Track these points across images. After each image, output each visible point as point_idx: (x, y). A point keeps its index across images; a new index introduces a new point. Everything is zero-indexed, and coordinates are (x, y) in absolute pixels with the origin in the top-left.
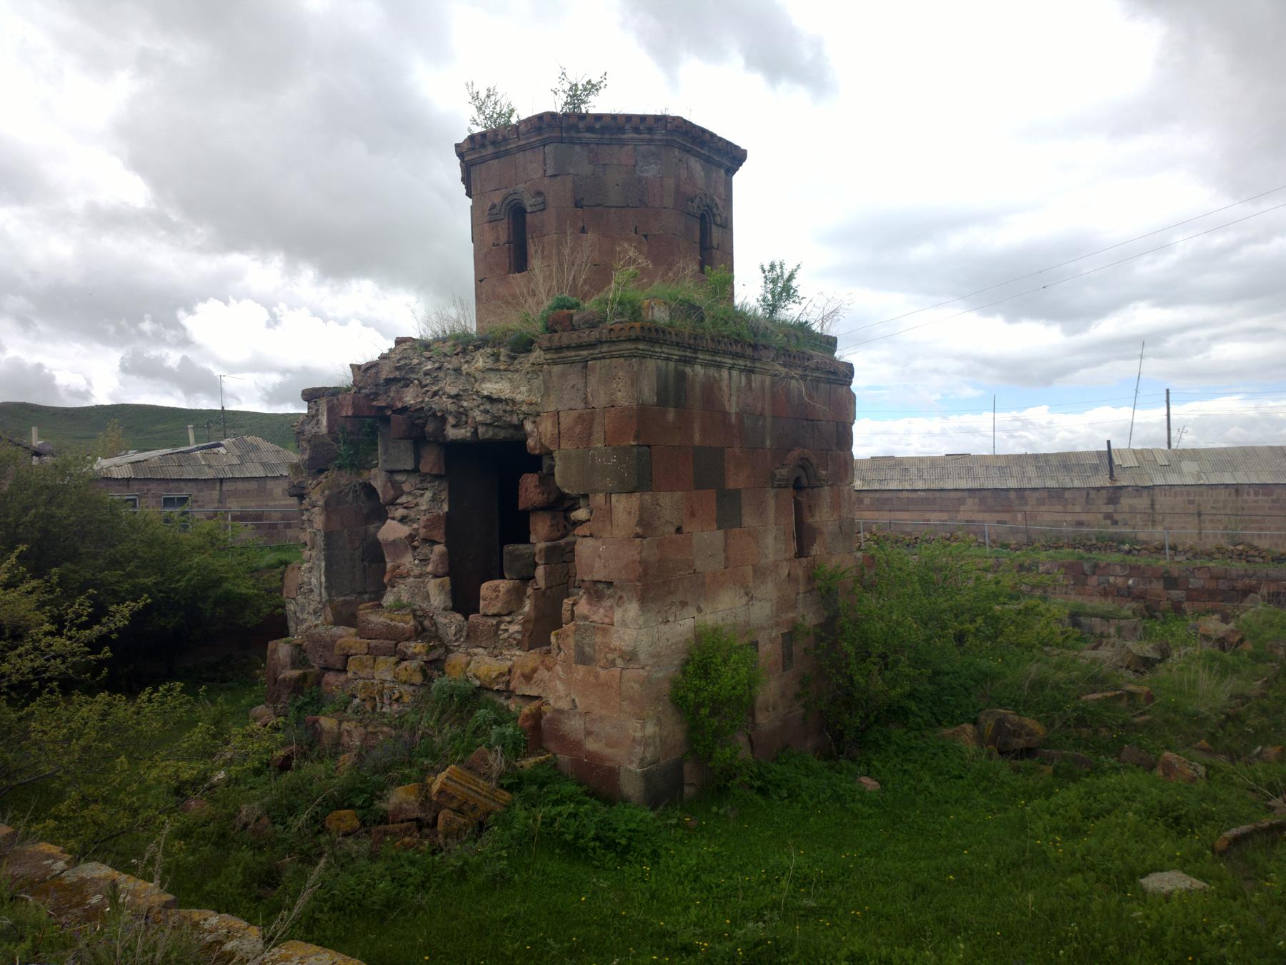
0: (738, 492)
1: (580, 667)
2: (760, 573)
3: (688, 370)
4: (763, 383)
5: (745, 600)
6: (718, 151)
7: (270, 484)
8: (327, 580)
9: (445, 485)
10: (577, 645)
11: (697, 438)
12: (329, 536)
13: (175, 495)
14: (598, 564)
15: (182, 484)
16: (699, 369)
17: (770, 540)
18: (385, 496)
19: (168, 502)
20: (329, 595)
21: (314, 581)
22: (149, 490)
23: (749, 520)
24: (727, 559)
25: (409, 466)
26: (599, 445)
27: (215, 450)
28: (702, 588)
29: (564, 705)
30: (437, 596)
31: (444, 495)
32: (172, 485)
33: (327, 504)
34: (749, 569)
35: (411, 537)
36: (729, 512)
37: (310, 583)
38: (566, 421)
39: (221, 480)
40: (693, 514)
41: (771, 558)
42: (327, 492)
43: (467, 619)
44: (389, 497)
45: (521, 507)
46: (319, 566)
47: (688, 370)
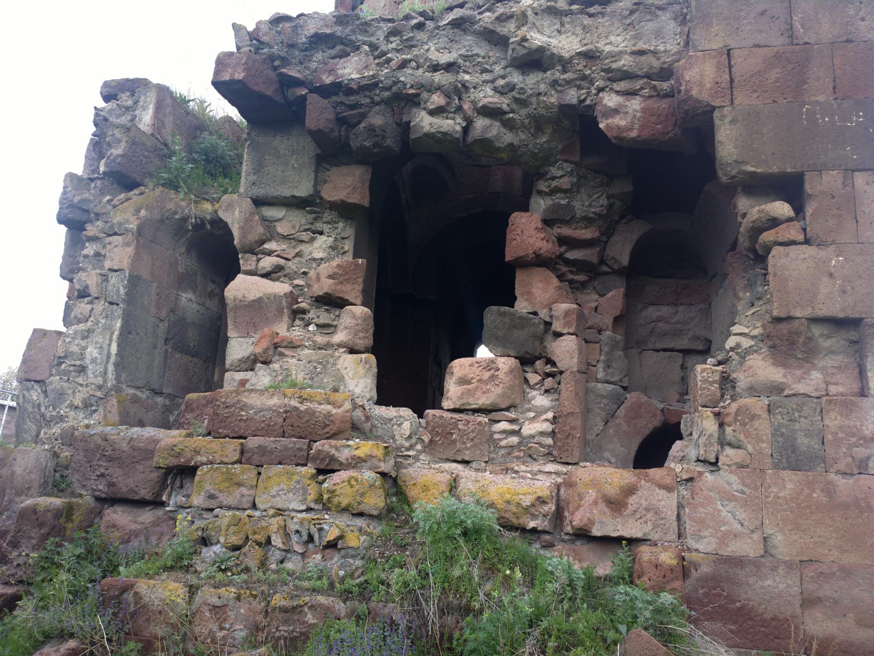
1: (787, 474)
8: (119, 354)
9: (350, 232)
10: (776, 432)
12: (134, 281)
14: (825, 288)
18: (243, 236)
20: (118, 378)
21: (92, 351)
25: (303, 190)
26: (821, 98)
29: (746, 547)
30: (358, 377)
31: (348, 246)
33: (140, 232)
35: (292, 298)
37: (82, 357)
38: (743, 64)
42: (143, 213)
43: (420, 416)
44: (253, 237)
45: (508, 258)
46: (108, 328)
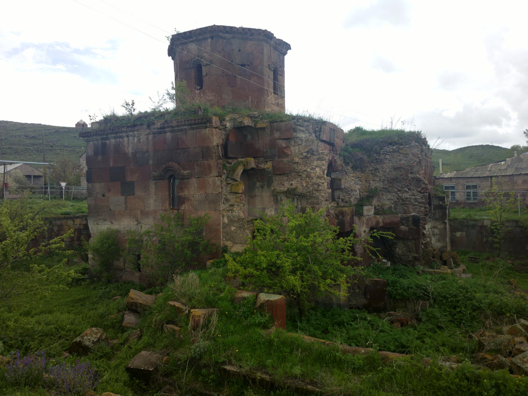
0: (132, 183)
2: (145, 214)
3: (107, 142)
4: (147, 139)
5: (136, 223)
6: (200, 34)
7: (515, 178)
11: (111, 164)
13: (471, 184)
15: (474, 179)
16: (113, 141)
17: (152, 201)
19: (468, 187)
22: (459, 182)
23: (138, 192)
24: (126, 207)
27: (499, 163)
28: (113, 216)
32: (469, 180)
34: (139, 211)
36: (127, 189)
39: (491, 177)
40: (109, 190)
41: (152, 208)
47: (107, 142)
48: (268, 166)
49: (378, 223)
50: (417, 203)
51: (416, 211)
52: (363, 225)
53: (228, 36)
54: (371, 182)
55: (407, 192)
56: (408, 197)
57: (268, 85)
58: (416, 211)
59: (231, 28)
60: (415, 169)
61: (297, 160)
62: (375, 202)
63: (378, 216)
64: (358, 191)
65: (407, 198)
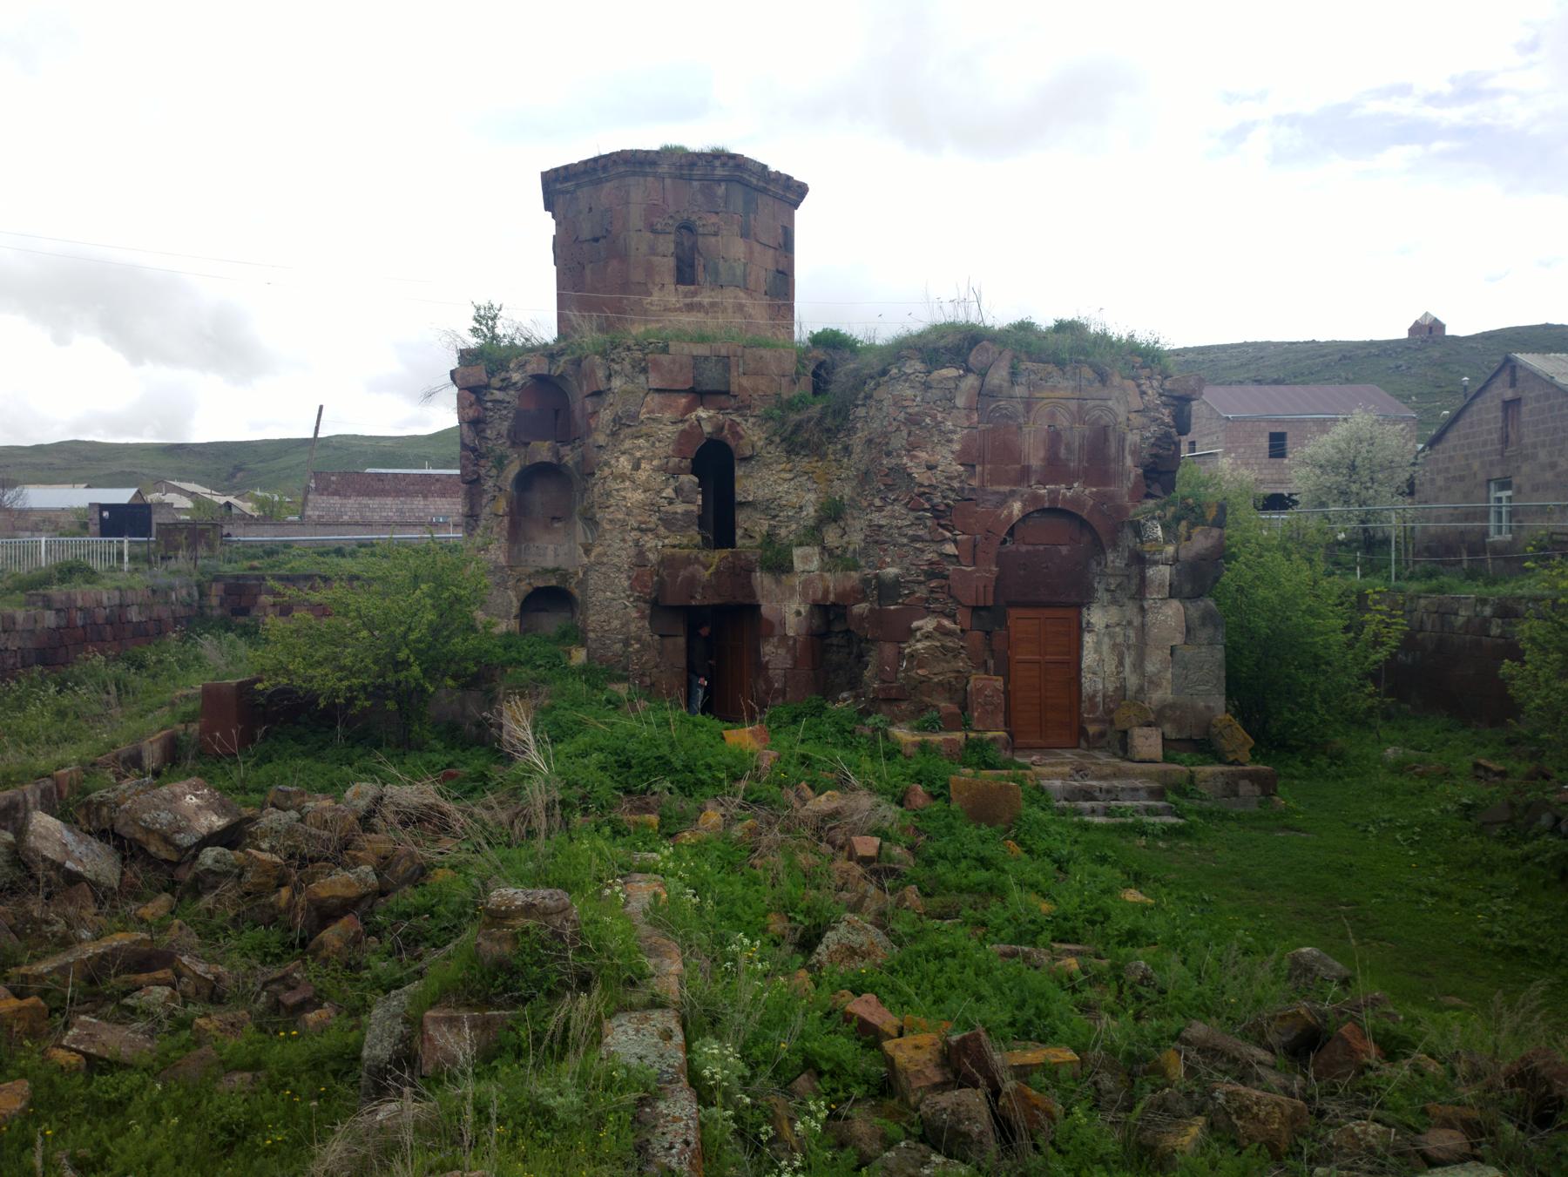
48: (569, 457)
49: (826, 592)
50: (905, 541)
51: (907, 561)
52: (792, 596)
53: (569, 185)
54: (836, 482)
55: (880, 509)
56: (883, 522)
57: (650, 270)
58: (907, 561)
59: (566, 168)
60: (898, 441)
61: (601, 439)
62: (831, 537)
63: (827, 575)
64: (811, 510)
65: (881, 527)
